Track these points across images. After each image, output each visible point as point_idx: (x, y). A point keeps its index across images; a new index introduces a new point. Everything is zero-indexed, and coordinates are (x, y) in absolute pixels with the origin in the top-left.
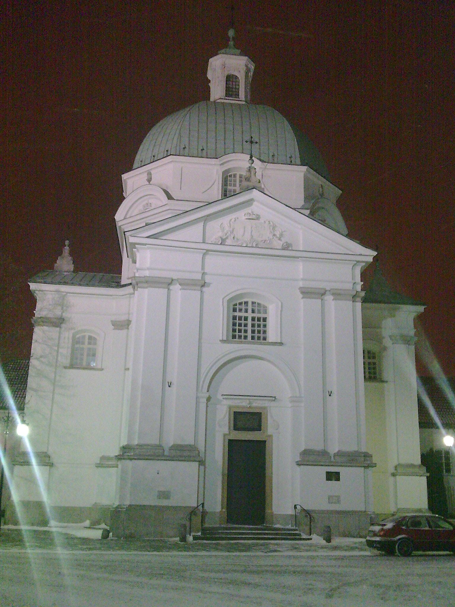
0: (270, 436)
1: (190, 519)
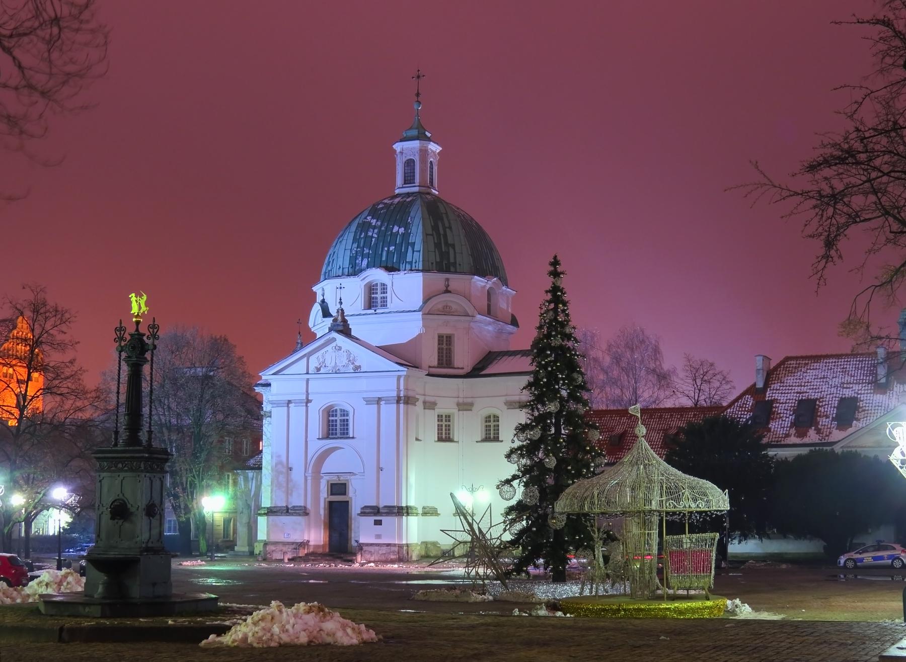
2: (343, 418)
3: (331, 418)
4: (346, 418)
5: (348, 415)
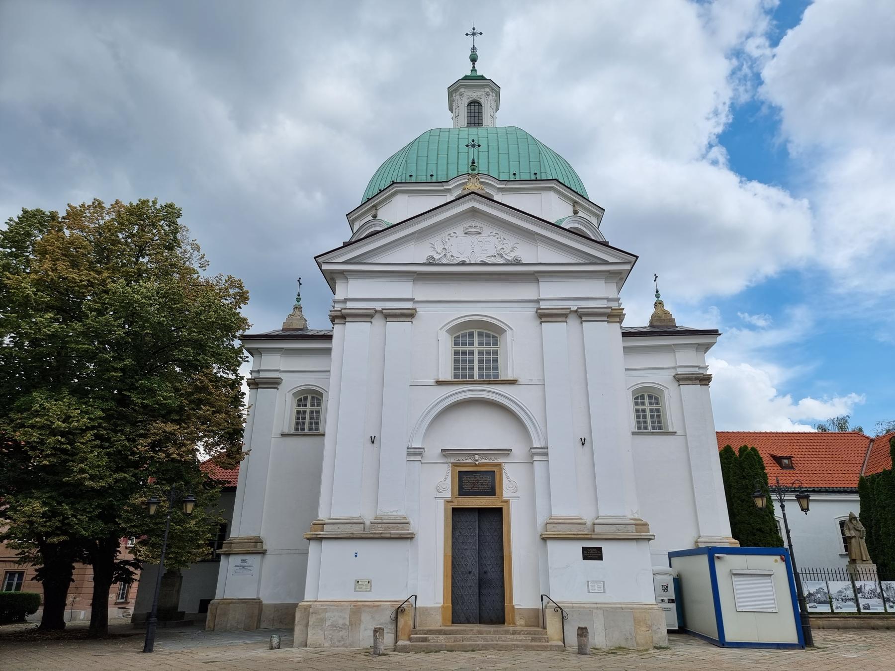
0: (507, 502)
1: (396, 618)
2: (484, 348)
4: (491, 348)
5: (495, 344)
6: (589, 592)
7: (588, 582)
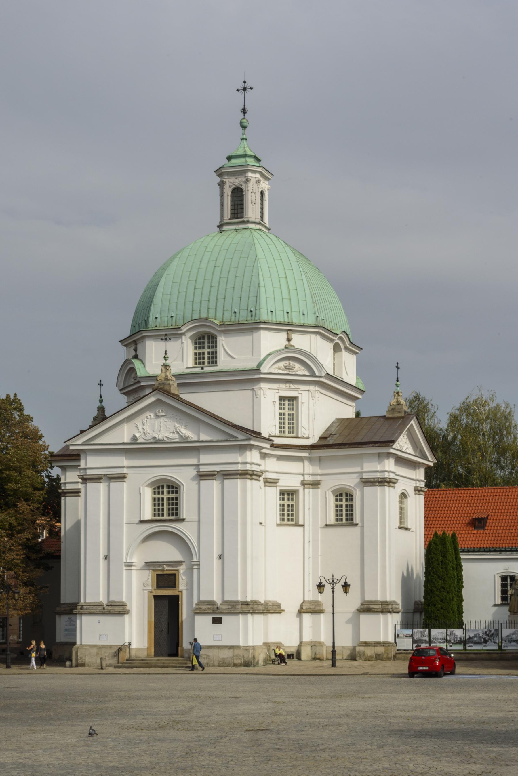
2: (171, 496)
3: (174, 496)
4: (174, 496)
6: (214, 640)
7: (214, 635)
